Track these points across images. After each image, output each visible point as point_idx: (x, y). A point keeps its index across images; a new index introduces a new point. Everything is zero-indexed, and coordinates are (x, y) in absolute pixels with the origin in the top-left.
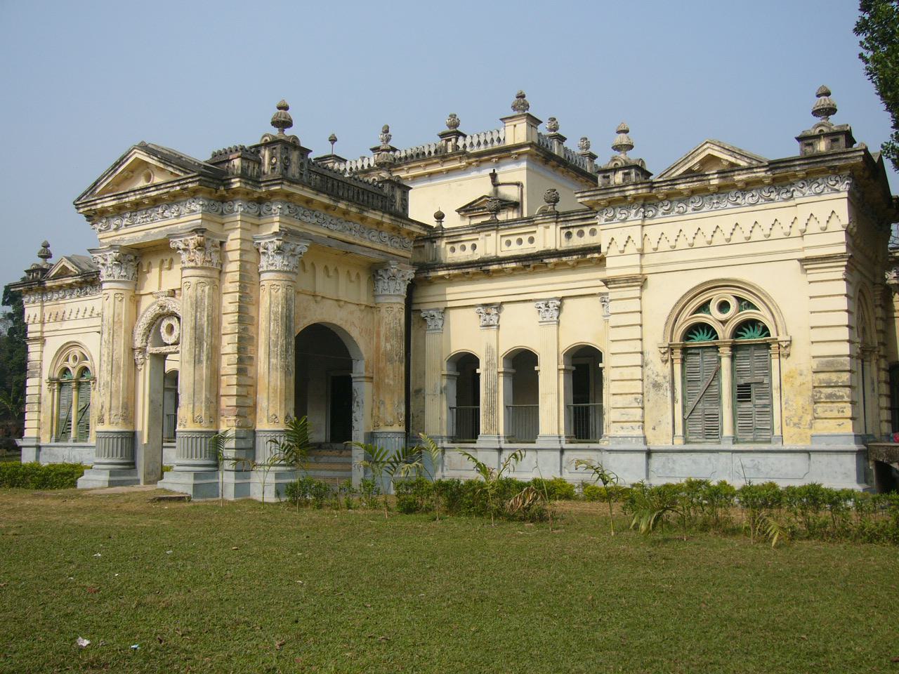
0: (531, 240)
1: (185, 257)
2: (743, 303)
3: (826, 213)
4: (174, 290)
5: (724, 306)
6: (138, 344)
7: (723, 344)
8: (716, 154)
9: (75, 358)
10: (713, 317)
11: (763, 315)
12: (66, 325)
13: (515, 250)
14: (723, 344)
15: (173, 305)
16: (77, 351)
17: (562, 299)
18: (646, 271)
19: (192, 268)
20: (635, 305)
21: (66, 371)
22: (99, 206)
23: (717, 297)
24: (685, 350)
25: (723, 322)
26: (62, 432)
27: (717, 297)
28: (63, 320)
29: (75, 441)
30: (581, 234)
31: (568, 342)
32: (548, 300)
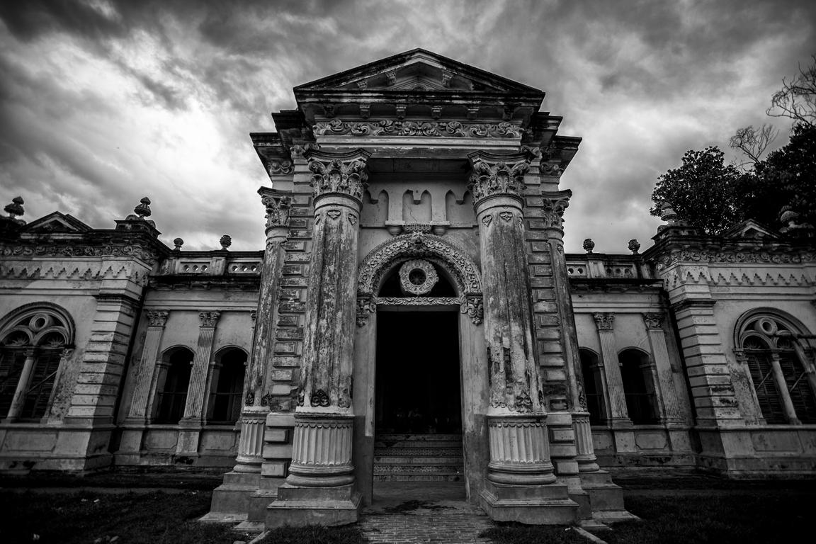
0: (581, 271)
1: (503, 183)
4: (434, 227)
6: (366, 290)
8: (756, 228)
15: (433, 245)
16: (46, 315)
17: (614, 313)
18: (715, 298)
19: (514, 197)
20: (710, 320)
22: (346, 100)
24: (747, 354)
25: (770, 337)
28: (32, 279)
29: (13, 422)
30: (618, 271)
32: (606, 314)
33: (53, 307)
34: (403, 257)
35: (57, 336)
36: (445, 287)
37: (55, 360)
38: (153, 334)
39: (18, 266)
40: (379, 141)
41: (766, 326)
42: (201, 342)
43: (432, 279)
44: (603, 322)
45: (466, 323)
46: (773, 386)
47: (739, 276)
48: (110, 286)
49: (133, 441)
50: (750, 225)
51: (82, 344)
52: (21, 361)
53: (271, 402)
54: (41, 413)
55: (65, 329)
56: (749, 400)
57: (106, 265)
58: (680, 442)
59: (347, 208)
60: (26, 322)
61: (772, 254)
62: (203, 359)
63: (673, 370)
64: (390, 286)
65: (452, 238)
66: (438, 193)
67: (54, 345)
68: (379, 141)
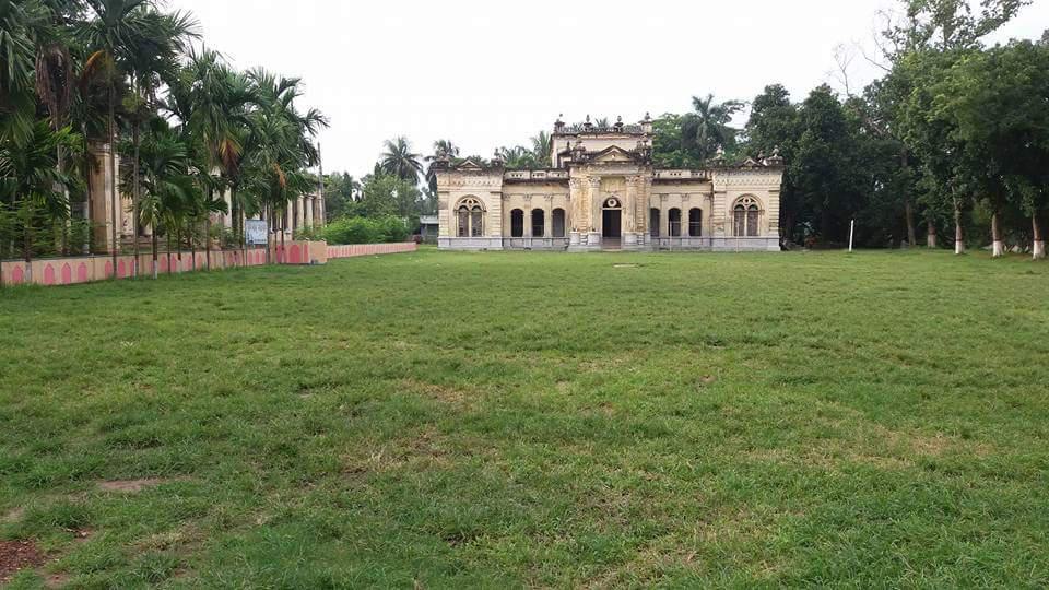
2: (752, 201)
3: (776, 180)
7: (746, 211)
10: (744, 203)
11: (757, 203)
13: (674, 177)
14: (746, 211)
21: (465, 207)
26: (462, 232)
31: (692, 206)
33: (473, 196)
35: (479, 207)
36: (619, 205)
37: (480, 215)
42: (526, 207)
43: (615, 203)
45: (622, 214)
46: (742, 223)
48: (494, 189)
49: (508, 243)
50: (750, 159)
52: (467, 216)
53: (582, 231)
54: (480, 234)
56: (729, 229)
57: (491, 181)
60: (465, 202)
63: (712, 216)
64: (606, 205)
66: (617, 182)
67: (478, 210)
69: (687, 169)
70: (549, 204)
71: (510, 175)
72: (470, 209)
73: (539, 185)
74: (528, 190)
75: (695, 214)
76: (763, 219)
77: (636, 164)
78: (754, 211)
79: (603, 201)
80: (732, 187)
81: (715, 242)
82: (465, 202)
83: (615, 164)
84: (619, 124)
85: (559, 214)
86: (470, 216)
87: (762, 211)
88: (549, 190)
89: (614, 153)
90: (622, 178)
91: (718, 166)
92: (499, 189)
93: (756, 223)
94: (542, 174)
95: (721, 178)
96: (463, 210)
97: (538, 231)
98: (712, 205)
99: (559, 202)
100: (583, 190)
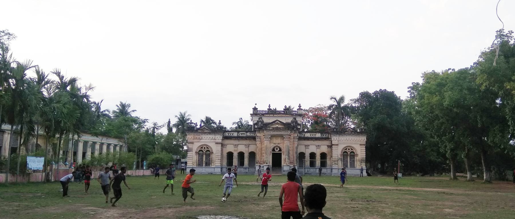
2: (352, 149)
3: (363, 139)
5: (349, 149)
9: (205, 148)
10: (347, 151)
11: (354, 151)
12: (202, 140)
14: (348, 155)
23: (348, 148)
26: (200, 164)
27: (348, 148)
33: (207, 145)
34: (275, 147)
35: (209, 151)
36: (280, 150)
38: (224, 149)
39: (198, 137)
40: (272, 133)
41: (349, 149)
42: (235, 151)
44: (318, 146)
46: (347, 161)
47: (345, 138)
48: (217, 141)
51: (214, 152)
52: (202, 156)
55: (210, 149)
57: (216, 137)
58: (329, 171)
59: (268, 142)
60: (202, 148)
61: (353, 134)
62: (235, 155)
64: (273, 150)
65: (281, 144)
68: (272, 133)
69: (319, 132)
70: (247, 149)
71: (227, 134)
72: (204, 152)
73: (244, 140)
74: (236, 142)
75: (323, 156)
76: (357, 158)
77: (288, 130)
78: (353, 155)
79: (272, 147)
80: (341, 142)
81: (333, 170)
82: (202, 148)
83: (277, 129)
84: (300, 109)
85: (252, 155)
86: (205, 155)
87: (357, 155)
88: (247, 142)
89: (277, 124)
90: (282, 136)
91: (334, 132)
92: (220, 141)
93: (354, 161)
94: (244, 134)
95: (335, 138)
96: (201, 152)
97: (241, 163)
98: (332, 149)
99: (252, 149)
100: (261, 143)
